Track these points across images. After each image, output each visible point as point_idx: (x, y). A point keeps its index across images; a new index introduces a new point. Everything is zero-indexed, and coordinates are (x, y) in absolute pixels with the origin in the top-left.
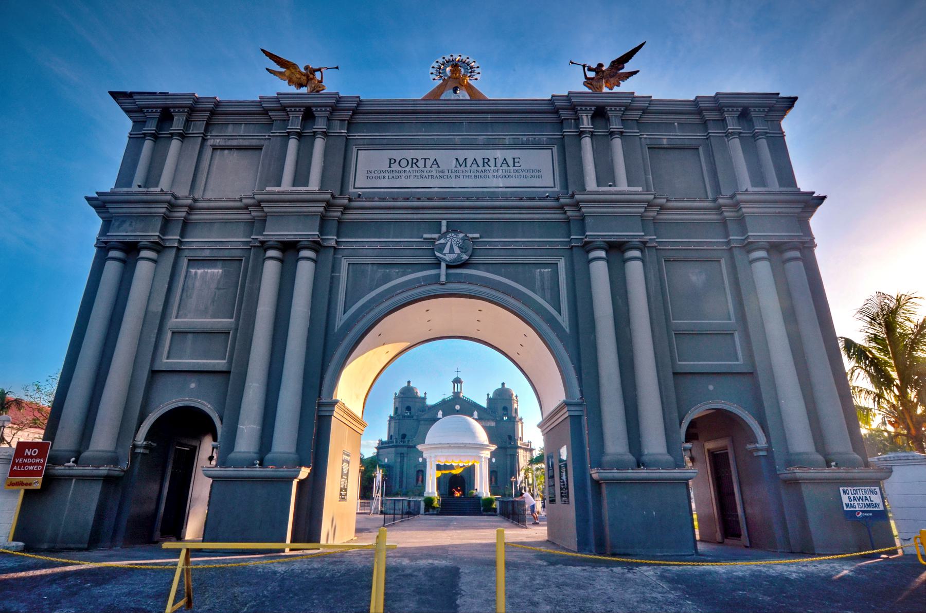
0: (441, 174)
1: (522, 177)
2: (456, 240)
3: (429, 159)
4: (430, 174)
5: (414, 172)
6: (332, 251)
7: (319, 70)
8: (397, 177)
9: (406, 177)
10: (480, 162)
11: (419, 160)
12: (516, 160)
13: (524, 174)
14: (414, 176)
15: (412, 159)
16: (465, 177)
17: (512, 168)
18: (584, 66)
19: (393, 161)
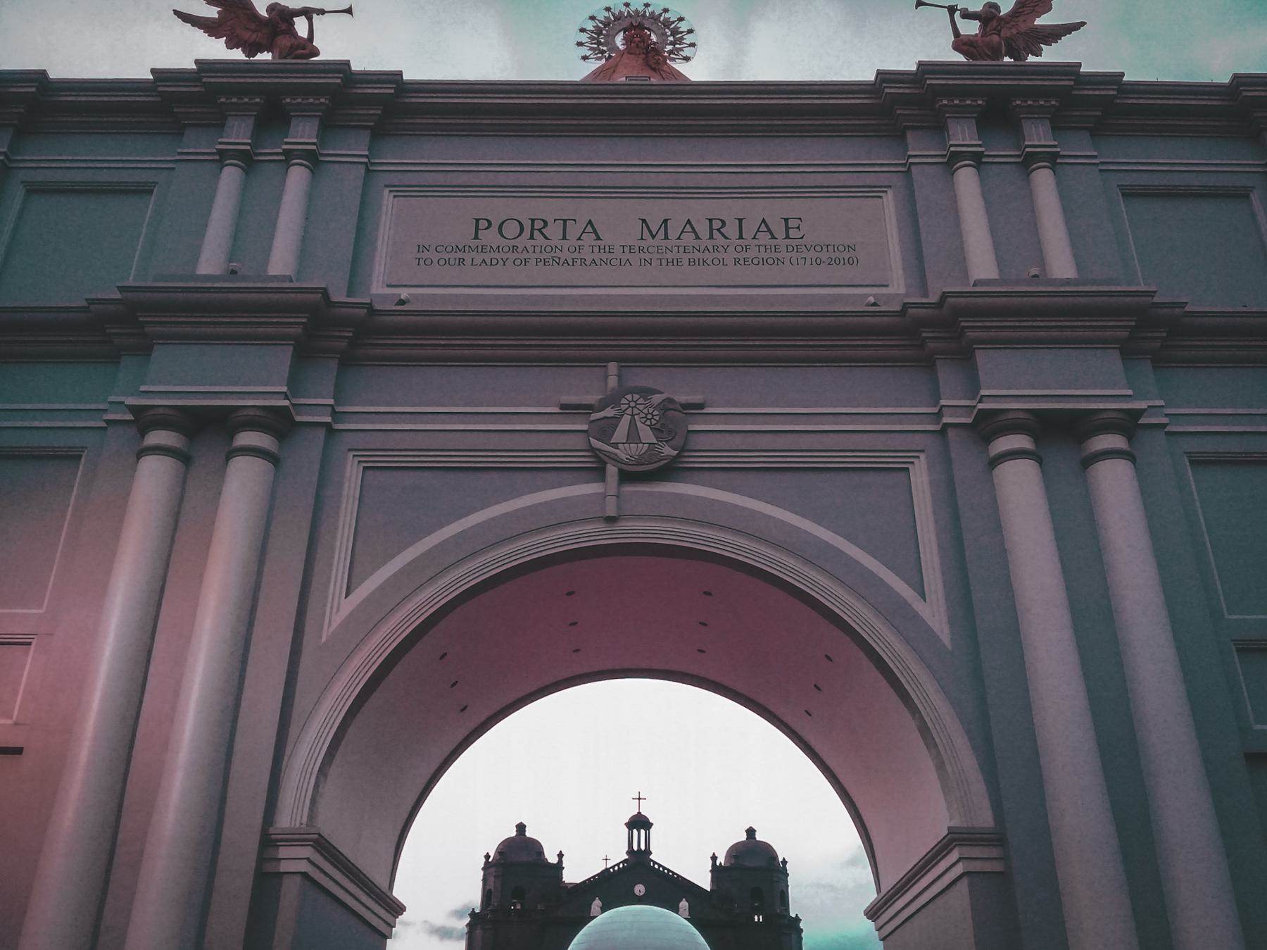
0: (604, 256)
1: (808, 261)
2: (646, 411)
3: (575, 220)
4: (575, 255)
5: (538, 249)
6: (321, 433)
7: (308, 13)
8: (494, 262)
9: (518, 262)
10: (703, 229)
12: (792, 223)
13: (813, 254)
14: (538, 260)
15: (533, 221)
16: (664, 262)
17: (781, 241)
18: (952, 10)
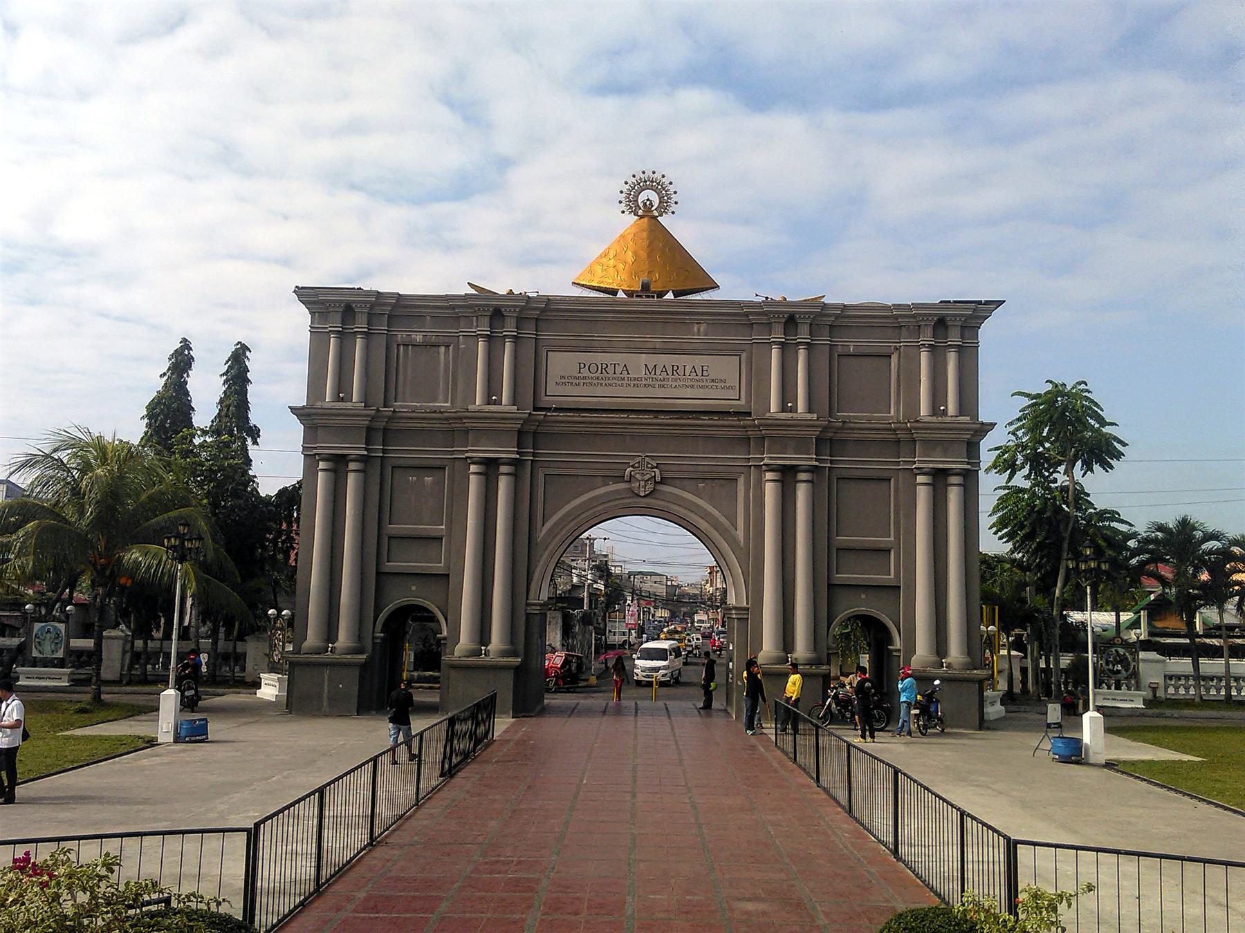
11: (609, 365)
12: (705, 368)
15: (602, 364)
17: (699, 377)
19: (582, 365)
